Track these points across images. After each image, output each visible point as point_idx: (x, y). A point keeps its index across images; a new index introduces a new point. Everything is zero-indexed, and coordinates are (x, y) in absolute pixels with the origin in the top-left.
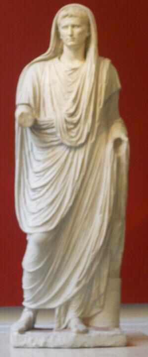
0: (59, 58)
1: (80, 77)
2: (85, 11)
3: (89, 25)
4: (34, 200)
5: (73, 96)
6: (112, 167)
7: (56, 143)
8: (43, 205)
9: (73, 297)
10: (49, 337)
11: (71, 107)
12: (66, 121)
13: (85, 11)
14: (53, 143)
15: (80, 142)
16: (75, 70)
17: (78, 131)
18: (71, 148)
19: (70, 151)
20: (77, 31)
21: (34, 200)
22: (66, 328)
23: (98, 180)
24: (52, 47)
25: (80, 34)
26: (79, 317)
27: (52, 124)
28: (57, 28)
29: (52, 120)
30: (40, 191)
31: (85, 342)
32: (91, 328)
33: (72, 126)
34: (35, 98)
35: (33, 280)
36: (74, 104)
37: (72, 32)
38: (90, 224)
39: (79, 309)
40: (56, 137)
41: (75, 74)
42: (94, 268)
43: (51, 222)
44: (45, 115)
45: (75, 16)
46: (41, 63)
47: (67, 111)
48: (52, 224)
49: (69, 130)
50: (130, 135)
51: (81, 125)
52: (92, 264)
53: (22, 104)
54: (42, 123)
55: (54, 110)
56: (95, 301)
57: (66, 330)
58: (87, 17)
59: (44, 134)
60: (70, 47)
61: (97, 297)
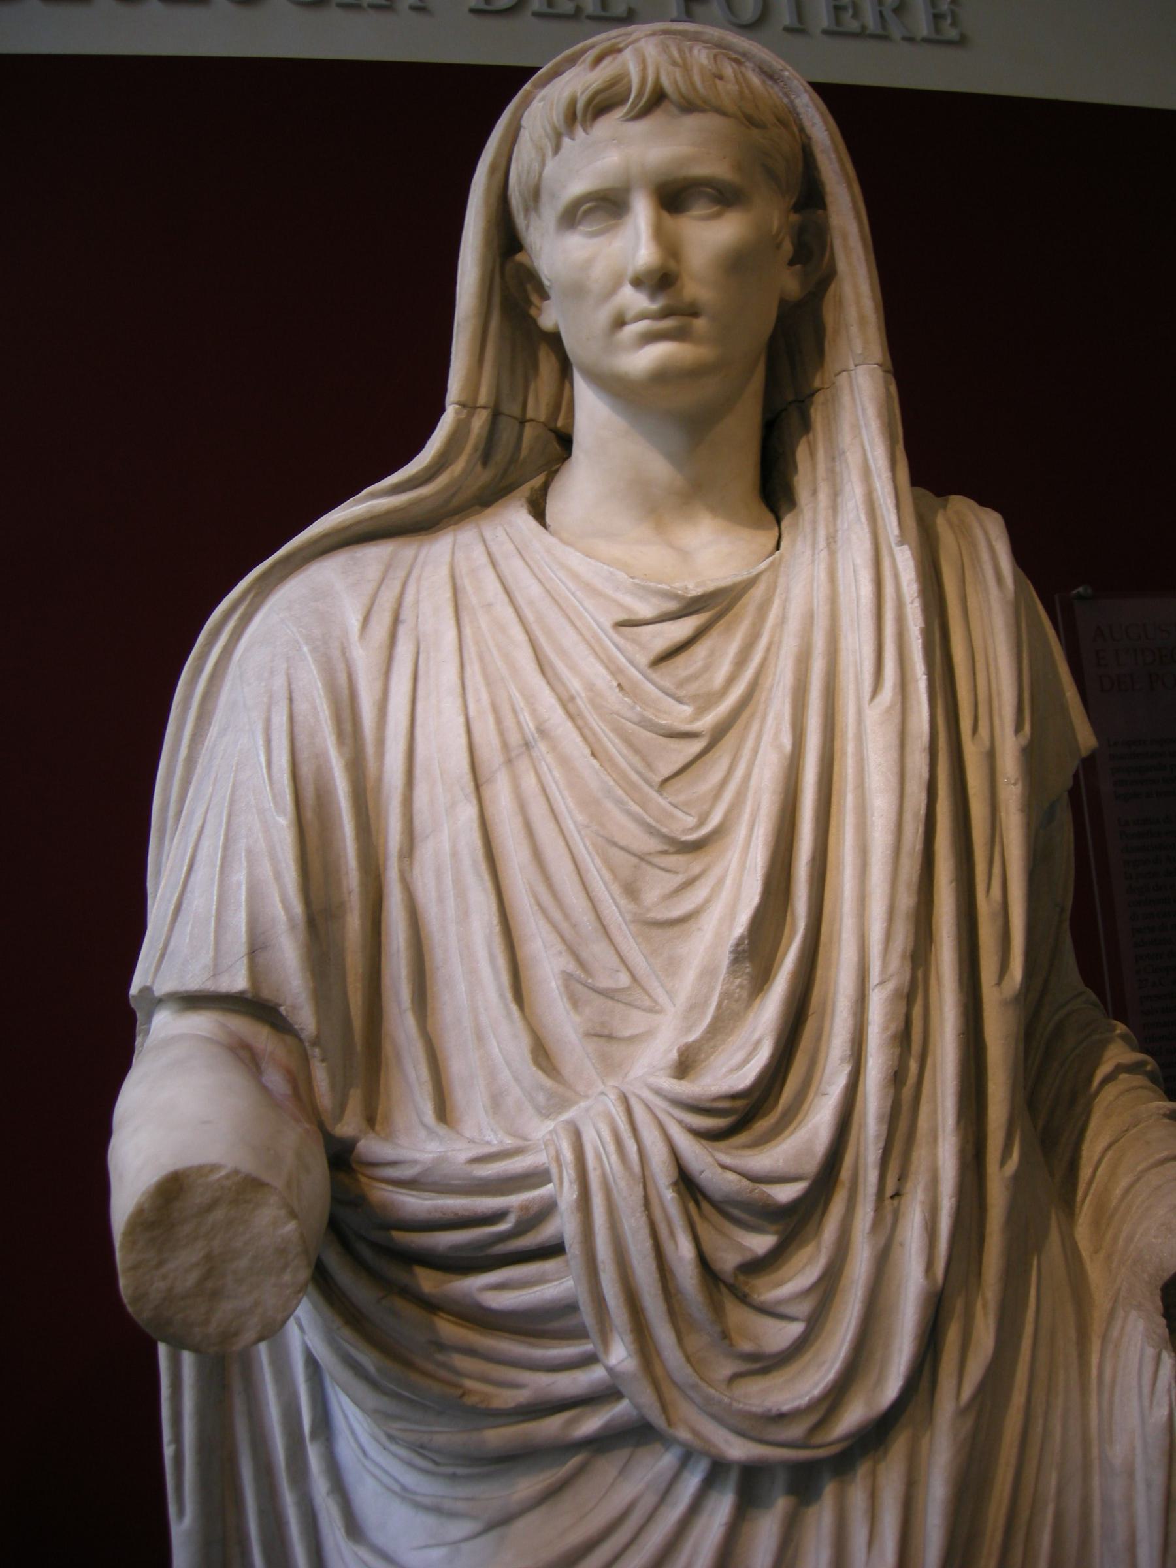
0: (538, 512)
7: (592, 1423)
11: (722, 1025)
14: (550, 1427)
24: (468, 406)
29: (537, 1177)
33: (761, 1243)
36: (761, 982)
37: (669, 245)
44: (444, 1111)
46: (375, 554)
47: (684, 1066)
53: (192, 1001)
54: (416, 1204)
59: (432, 1306)
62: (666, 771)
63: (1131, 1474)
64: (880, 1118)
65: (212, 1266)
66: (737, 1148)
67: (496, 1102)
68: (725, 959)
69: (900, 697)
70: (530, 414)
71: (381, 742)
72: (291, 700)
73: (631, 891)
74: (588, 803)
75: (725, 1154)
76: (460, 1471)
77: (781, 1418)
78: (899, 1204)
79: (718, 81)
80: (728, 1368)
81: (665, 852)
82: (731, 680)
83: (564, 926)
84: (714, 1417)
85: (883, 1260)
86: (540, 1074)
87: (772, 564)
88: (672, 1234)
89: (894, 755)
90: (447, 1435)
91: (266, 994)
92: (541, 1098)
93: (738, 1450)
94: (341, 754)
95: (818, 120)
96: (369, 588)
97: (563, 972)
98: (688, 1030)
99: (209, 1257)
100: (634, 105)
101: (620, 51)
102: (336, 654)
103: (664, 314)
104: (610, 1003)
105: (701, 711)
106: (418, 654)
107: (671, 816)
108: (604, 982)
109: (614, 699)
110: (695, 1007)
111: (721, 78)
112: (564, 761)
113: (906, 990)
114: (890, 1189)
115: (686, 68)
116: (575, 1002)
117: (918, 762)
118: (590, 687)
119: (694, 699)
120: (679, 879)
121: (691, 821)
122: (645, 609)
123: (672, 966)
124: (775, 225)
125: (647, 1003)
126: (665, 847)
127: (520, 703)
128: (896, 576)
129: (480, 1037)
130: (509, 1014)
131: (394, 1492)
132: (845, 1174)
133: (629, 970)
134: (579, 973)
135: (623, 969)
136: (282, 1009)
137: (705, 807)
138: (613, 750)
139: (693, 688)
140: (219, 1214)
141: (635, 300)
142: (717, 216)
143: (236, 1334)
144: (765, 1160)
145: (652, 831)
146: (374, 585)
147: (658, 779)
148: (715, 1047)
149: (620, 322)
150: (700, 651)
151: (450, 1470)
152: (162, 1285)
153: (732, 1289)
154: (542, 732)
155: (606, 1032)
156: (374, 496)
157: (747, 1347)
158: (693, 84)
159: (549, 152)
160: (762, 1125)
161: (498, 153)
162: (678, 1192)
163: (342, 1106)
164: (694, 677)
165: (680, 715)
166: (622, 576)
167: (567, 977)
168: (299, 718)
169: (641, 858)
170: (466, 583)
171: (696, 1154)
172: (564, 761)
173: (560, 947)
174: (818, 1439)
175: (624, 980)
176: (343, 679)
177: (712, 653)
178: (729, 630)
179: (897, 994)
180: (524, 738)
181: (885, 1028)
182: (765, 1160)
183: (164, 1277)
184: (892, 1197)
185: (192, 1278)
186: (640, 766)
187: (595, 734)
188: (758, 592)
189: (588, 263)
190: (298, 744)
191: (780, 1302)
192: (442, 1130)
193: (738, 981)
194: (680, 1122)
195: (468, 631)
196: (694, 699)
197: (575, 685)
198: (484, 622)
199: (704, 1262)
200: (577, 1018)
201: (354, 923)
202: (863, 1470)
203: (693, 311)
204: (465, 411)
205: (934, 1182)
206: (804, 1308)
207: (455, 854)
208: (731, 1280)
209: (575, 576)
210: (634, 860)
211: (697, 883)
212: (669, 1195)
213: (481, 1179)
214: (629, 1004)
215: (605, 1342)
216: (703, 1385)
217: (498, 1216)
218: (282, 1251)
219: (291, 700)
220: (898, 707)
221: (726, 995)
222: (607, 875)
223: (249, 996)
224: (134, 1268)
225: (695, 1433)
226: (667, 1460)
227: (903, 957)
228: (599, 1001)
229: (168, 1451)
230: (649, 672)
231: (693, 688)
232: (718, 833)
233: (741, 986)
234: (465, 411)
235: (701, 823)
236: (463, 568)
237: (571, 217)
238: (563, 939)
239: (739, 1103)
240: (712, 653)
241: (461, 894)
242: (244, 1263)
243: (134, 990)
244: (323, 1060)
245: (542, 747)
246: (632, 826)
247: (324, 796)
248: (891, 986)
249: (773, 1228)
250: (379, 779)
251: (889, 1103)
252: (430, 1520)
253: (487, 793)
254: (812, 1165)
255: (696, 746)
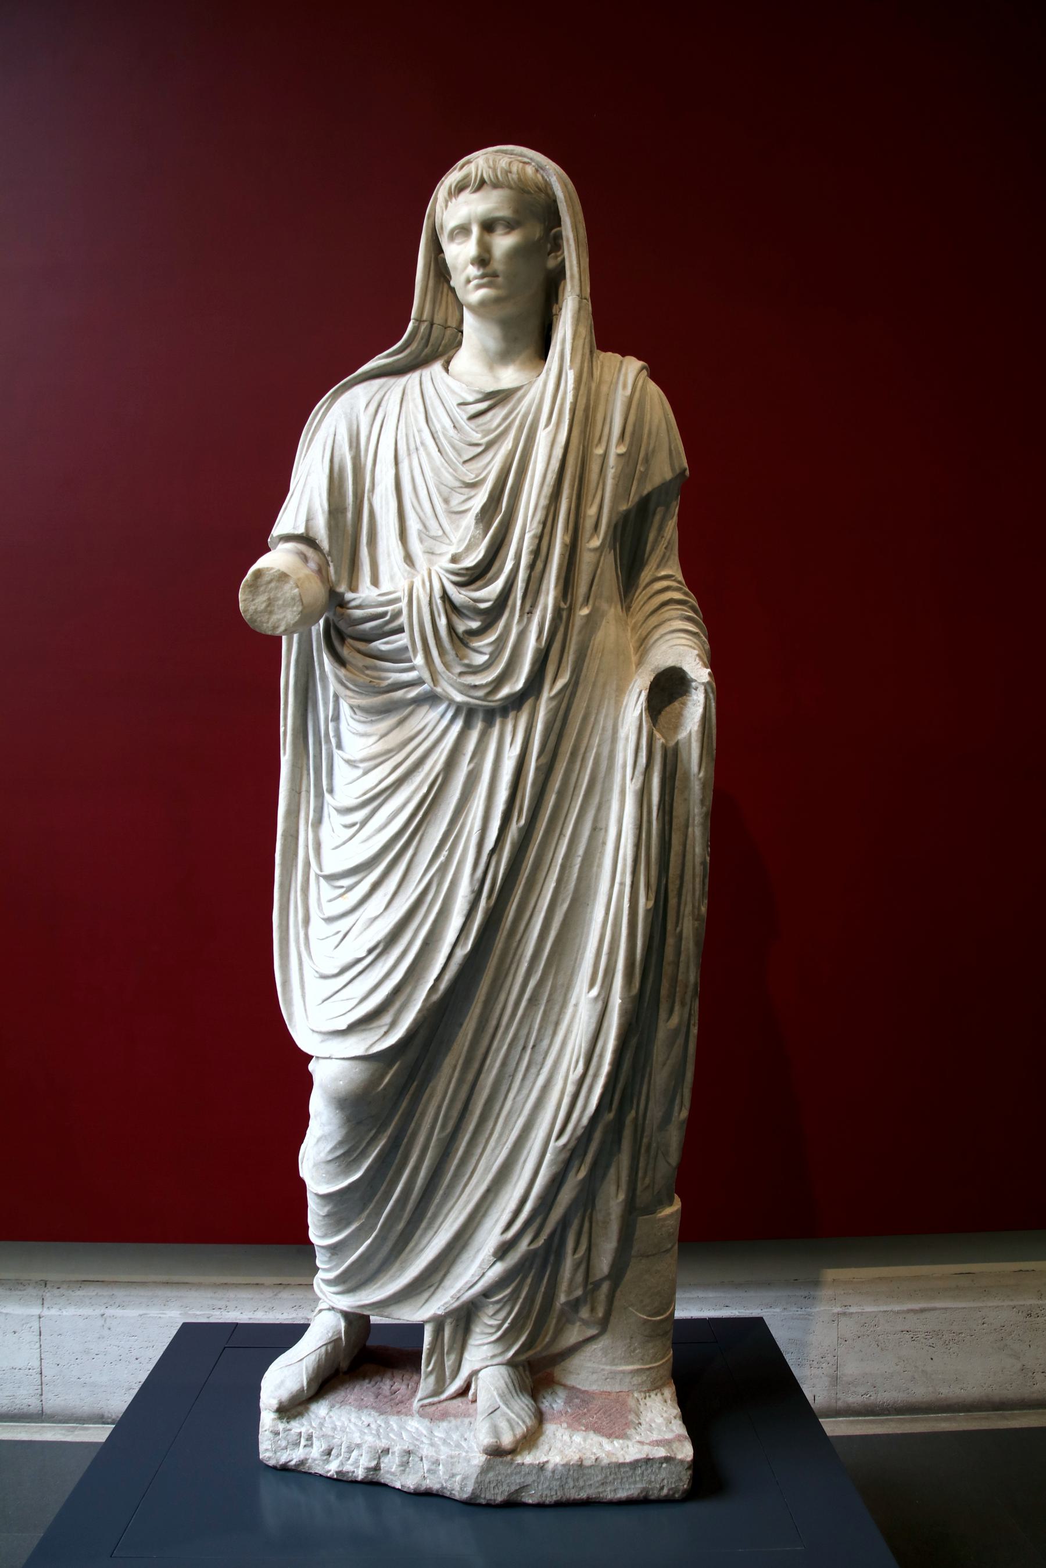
1: (517, 423)
2: (539, 168)
3: (551, 216)
4: (330, 920)
5: (481, 497)
6: (643, 794)
7: (413, 693)
8: (359, 945)
9: (486, 1294)
10: (386, 1451)
11: (469, 548)
12: (445, 597)
13: (539, 168)
14: (399, 694)
15: (505, 691)
16: (498, 398)
17: (501, 642)
18: (468, 714)
19: (467, 726)
20: (503, 243)
21: (330, 920)
22: (464, 1392)
23: (581, 851)
24: (419, 321)
25: (515, 254)
26: (511, 1363)
27: (397, 614)
28: (437, 249)
30: (350, 888)
31: (523, 1488)
32: (555, 1403)
33: (475, 625)
34: (335, 511)
35: (337, 1219)
38: (552, 1021)
39: (505, 1339)
40: (413, 668)
41: (500, 413)
42: (566, 1196)
43: (387, 1019)
44: (375, 582)
45: (496, 186)
47: (454, 559)
48: (393, 1025)
49: (461, 640)
50: (715, 661)
51: (511, 621)
52: (556, 1183)
54: (358, 613)
55: (409, 559)
56: (575, 1305)
57: (458, 1402)
58: (546, 190)
60: (482, 309)
61: (579, 1292)
62: (466, 458)
63: (627, 739)
64: (523, 581)
65: (270, 602)
66: (470, 590)
67: (392, 578)
68: (473, 522)
69: (555, 428)
70: (449, 324)
71: (367, 450)
72: (335, 435)
73: (446, 501)
74: (436, 471)
75: (463, 591)
76: (373, 719)
77: (475, 687)
78: (531, 617)
79: (509, 174)
80: (459, 669)
81: (461, 487)
82: (499, 425)
83: (421, 514)
84: (452, 685)
85: (522, 635)
86: (406, 565)
87: (530, 382)
88: (439, 616)
89: (548, 449)
90: (365, 701)
91: (311, 534)
92: (406, 575)
93: (459, 698)
94: (350, 454)
95: (559, 188)
96: (371, 394)
97: (418, 530)
98: (458, 548)
99: (269, 599)
100: (472, 189)
101: (471, 162)
102: (355, 418)
103: (483, 276)
104: (434, 541)
105: (484, 436)
106: (384, 417)
107: (466, 475)
108: (433, 533)
109: (452, 432)
110: (461, 541)
111: (510, 172)
112: (428, 454)
113: (539, 535)
114: (527, 608)
115: (494, 170)
116: (421, 541)
117: (558, 452)
118: (444, 428)
119: (482, 431)
120: (465, 497)
121: (473, 476)
122: (471, 399)
123: (458, 527)
124: (537, 236)
125: (448, 541)
126: (461, 485)
127: (416, 434)
128: (566, 382)
129: (389, 555)
130: (398, 547)
131: (354, 733)
132: (510, 602)
133: (442, 529)
134: (424, 530)
135: (440, 529)
136: (317, 541)
137: (480, 471)
138: (448, 450)
139: (483, 428)
140: (273, 585)
141: (473, 271)
142: (508, 233)
143: (278, 627)
144: (477, 595)
145: (457, 479)
146: (374, 393)
147: (461, 461)
148: (467, 556)
149: (468, 281)
150: (490, 415)
151: (369, 719)
152: (253, 607)
153: (461, 640)
154: (422, 444)
155: (431, 551)
156: (380, 359)
157: (466, 661)
158: (497, 176)
159: (444, 209)
160: (479, 583)
161: (431, 209)
162: (444, 602)
163: (339, 582)
164: (485, 424)
165: (476, 437)
166: (464, 386)
167: (419, 532)
168: (337, 442)
169: (452, 489)
170: (408, 391)
171: (452, 590)
172: (428, 454)
173: (418, 520)
174: (490, 698)
175: (440, 533)
176: (355, 427)
177: (494, 415)
178: (504, 406)
179: (534, 536)
180: (416, 446)
181: (528, 548)
182: (477, 595)
183: (254, 605)
184: (528, 613)
185: (264, 605)
186: (456, 456)
187: (442, 444)
188: (520, 393)
189: (458, 255)
190: (335, 451)
191: (480, 647)
192: (373, 588)
193: (478, 532)
194: (448, 579)
195: (404, 409)
196: (482, 431)
197: (438, 427)
198: (411, 405)
199: (451, 628)
200: (421, 546)
201: (349, 515)
202: (512, 715)
203: (495, 275)
204: (417, 322)
205: (545, 608)
206: (489, 650)
207: (386, 489)
208: (462, 636)
209: (448, 387)
210: (450, 490)
211: (472, 499)
212: (439, 601)
213: (381, 601)
214: (441, 542)
215: (415, 656)
216: (447, 672)
217: (383, 615)
218: (293, 599)
219: (335, 435)
220: (553, 432)
221: (473, 536)
222: (438, 495)
223: (305, 535)
224: (245, 600)
225: (443, 690)
226: (442, 708)
227: (539, 522)
228: (431, 541)
229: (282, 729)
230: (468, 423)
231: (483, 428)
232: (482, 481)
233: (479, 534)
234: (417, 322)
235: (477, 476)
236: (409, 386)
237: (452, 236)
238: (420, 518)
239: (469, 572)
240: (494, 415)
241: (387, 503)
242: (280, 602)
243: (269, 540)
244: (332, 562)
245: (421, 450)
246: (450, 478)
247: (342, 470)
248: (532, 533)
249: (477, 618)
250: (365, 465)
251: (527, 575)
252: (364, 740)
253: (401, 466)
254: (494, 596)
255: (480, 449)
